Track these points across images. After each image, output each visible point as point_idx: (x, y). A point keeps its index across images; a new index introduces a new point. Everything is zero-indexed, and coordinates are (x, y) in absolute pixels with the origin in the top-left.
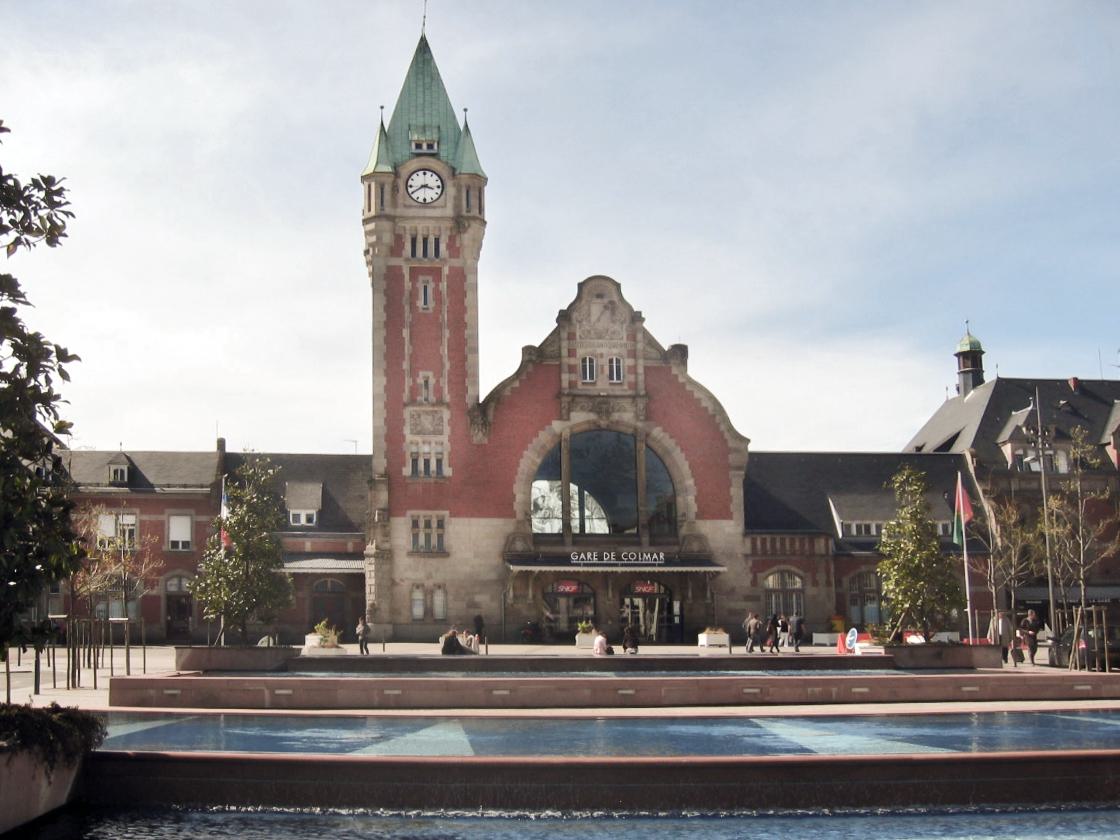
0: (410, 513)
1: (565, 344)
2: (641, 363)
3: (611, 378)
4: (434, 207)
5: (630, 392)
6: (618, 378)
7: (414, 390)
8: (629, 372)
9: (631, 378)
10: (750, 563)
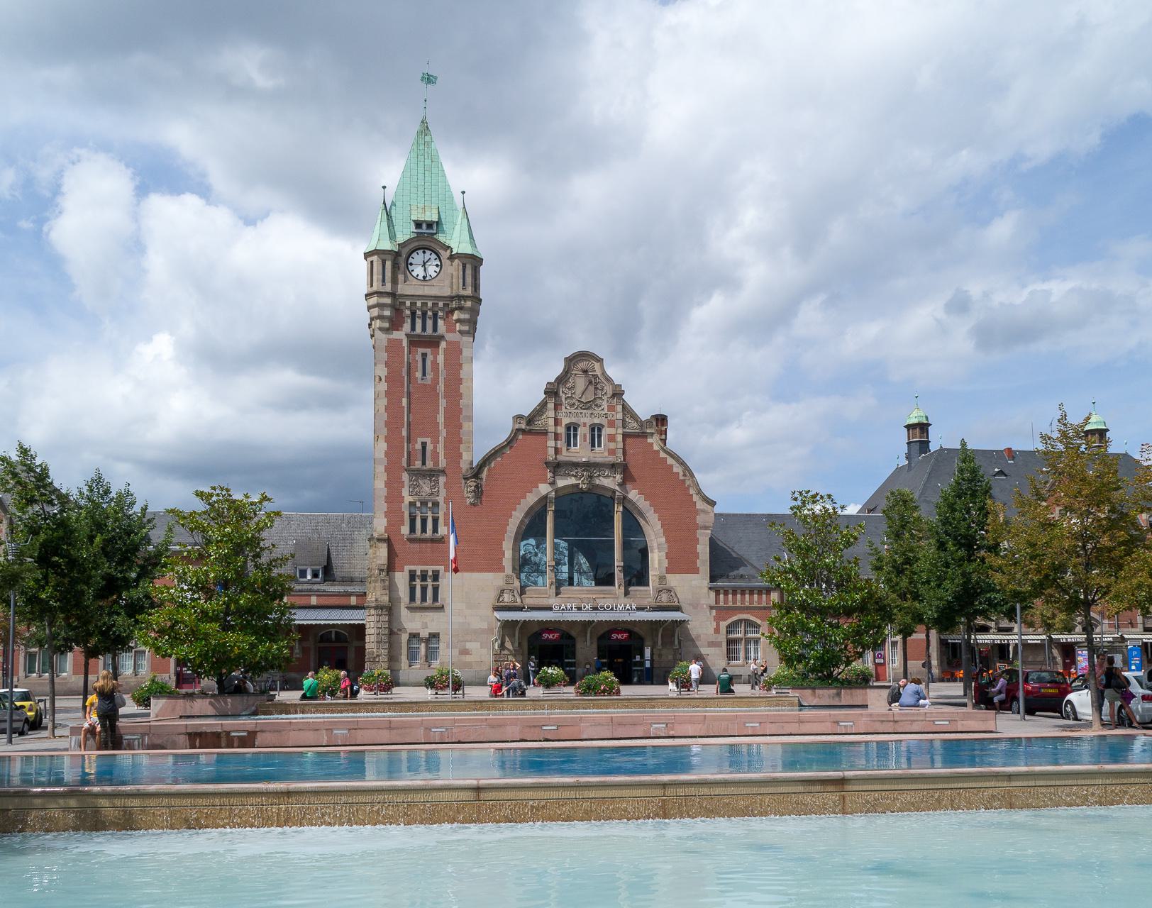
0: (407, 568)
2: (620, 431)
3: (593, 445)
5: (611, 459)
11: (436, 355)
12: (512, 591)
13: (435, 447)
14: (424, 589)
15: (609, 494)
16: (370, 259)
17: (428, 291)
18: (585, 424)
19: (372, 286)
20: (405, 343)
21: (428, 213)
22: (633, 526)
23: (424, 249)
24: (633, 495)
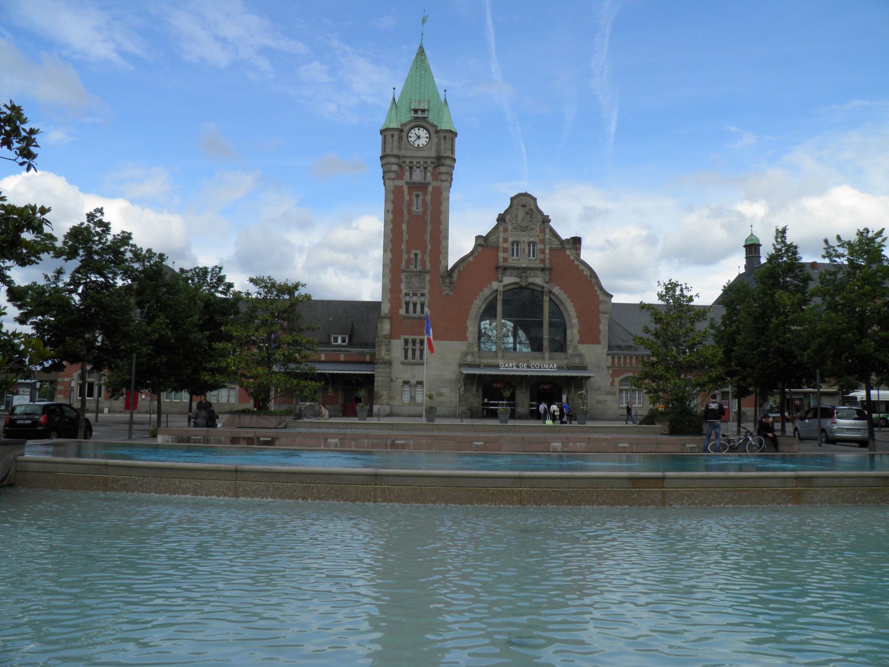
0: (403, 337)
1: (501, 235)
2: (548, 247)
3: (529, 256)
4: (424, 150)
5: (541, 265)
6: (534, 256)
7: (408, 262)
8: (540, 253)
9: (542, 256)
10: (611, 372)
11: (425, 194)
12: (473, 354)
13: (423, 257)
14: (414, 351)
15: (539, 289)
16: (384, 134)
17: (421, 154)
18: (524, 242)
19: (385, 151)
20: (406, 188)
21: (422, 104)
22: (557, 311)
23: (419, 127)
24: (556, 290)
